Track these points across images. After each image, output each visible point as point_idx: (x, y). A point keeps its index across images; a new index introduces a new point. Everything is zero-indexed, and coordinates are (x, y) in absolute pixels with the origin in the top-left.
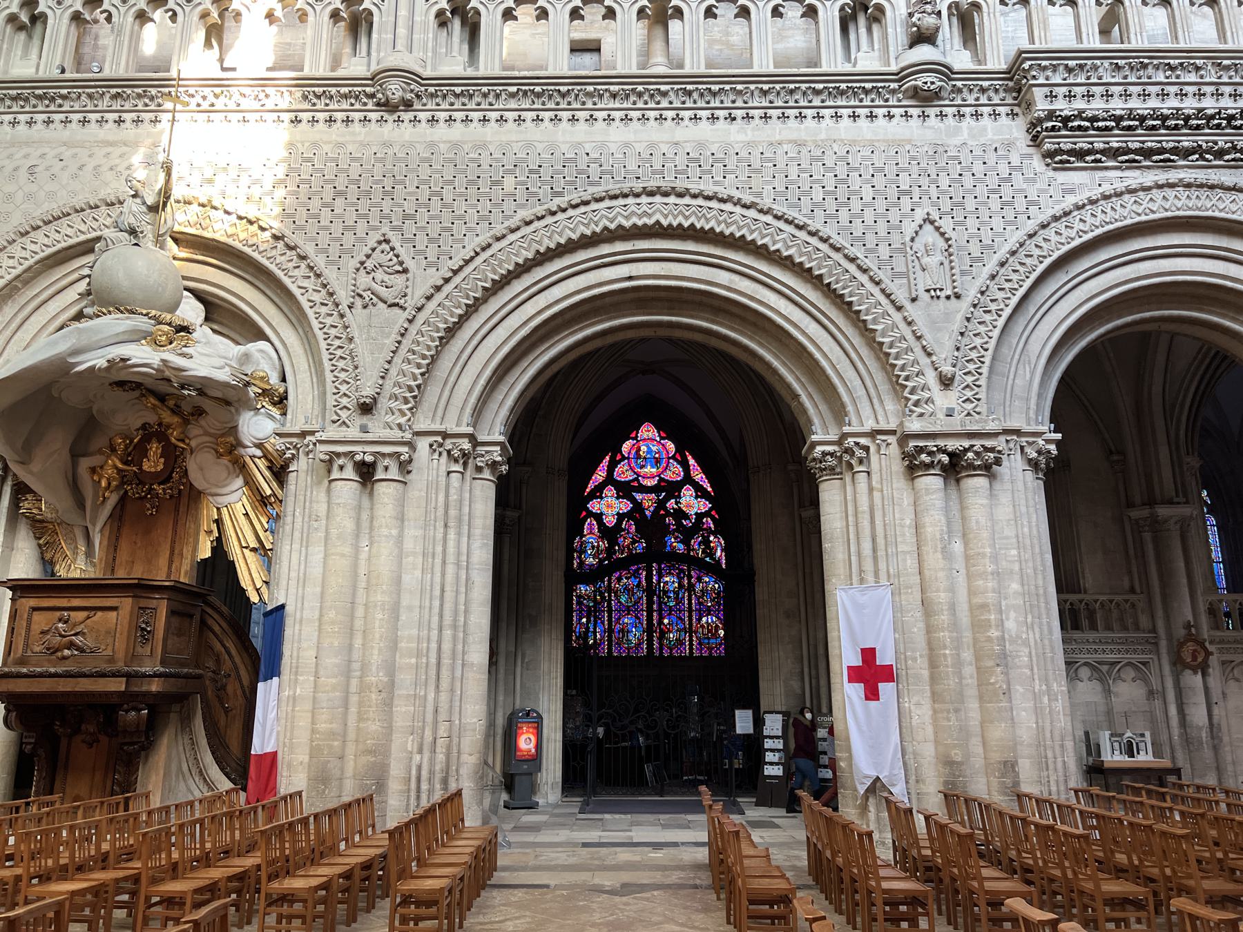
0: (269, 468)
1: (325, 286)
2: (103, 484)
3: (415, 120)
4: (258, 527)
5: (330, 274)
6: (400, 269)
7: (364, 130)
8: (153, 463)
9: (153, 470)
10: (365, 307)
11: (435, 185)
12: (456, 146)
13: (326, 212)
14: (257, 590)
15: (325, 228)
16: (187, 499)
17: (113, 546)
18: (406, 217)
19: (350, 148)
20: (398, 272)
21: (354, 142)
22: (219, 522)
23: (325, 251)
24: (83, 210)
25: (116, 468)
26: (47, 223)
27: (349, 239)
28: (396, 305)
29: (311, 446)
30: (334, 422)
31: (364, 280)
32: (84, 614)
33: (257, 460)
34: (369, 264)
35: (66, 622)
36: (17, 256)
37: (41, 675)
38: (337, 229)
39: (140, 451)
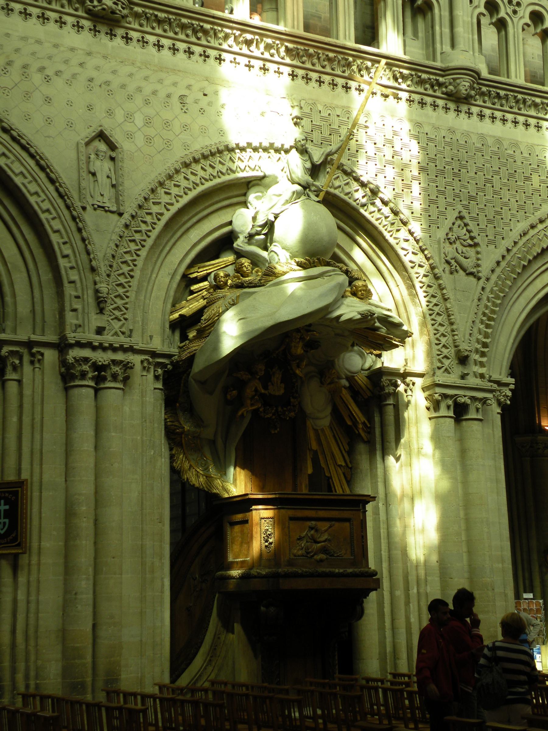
3: (470, 114)
6: (472, 243)
7: (434, 114)
9: (277, 394)
12: (499, 141)
18: (471, 198)
20: (470, 246)
21: (429, 124)
26: (205, 157)
28: (471, 274)
30: (439, 368)
31: (450, 249)
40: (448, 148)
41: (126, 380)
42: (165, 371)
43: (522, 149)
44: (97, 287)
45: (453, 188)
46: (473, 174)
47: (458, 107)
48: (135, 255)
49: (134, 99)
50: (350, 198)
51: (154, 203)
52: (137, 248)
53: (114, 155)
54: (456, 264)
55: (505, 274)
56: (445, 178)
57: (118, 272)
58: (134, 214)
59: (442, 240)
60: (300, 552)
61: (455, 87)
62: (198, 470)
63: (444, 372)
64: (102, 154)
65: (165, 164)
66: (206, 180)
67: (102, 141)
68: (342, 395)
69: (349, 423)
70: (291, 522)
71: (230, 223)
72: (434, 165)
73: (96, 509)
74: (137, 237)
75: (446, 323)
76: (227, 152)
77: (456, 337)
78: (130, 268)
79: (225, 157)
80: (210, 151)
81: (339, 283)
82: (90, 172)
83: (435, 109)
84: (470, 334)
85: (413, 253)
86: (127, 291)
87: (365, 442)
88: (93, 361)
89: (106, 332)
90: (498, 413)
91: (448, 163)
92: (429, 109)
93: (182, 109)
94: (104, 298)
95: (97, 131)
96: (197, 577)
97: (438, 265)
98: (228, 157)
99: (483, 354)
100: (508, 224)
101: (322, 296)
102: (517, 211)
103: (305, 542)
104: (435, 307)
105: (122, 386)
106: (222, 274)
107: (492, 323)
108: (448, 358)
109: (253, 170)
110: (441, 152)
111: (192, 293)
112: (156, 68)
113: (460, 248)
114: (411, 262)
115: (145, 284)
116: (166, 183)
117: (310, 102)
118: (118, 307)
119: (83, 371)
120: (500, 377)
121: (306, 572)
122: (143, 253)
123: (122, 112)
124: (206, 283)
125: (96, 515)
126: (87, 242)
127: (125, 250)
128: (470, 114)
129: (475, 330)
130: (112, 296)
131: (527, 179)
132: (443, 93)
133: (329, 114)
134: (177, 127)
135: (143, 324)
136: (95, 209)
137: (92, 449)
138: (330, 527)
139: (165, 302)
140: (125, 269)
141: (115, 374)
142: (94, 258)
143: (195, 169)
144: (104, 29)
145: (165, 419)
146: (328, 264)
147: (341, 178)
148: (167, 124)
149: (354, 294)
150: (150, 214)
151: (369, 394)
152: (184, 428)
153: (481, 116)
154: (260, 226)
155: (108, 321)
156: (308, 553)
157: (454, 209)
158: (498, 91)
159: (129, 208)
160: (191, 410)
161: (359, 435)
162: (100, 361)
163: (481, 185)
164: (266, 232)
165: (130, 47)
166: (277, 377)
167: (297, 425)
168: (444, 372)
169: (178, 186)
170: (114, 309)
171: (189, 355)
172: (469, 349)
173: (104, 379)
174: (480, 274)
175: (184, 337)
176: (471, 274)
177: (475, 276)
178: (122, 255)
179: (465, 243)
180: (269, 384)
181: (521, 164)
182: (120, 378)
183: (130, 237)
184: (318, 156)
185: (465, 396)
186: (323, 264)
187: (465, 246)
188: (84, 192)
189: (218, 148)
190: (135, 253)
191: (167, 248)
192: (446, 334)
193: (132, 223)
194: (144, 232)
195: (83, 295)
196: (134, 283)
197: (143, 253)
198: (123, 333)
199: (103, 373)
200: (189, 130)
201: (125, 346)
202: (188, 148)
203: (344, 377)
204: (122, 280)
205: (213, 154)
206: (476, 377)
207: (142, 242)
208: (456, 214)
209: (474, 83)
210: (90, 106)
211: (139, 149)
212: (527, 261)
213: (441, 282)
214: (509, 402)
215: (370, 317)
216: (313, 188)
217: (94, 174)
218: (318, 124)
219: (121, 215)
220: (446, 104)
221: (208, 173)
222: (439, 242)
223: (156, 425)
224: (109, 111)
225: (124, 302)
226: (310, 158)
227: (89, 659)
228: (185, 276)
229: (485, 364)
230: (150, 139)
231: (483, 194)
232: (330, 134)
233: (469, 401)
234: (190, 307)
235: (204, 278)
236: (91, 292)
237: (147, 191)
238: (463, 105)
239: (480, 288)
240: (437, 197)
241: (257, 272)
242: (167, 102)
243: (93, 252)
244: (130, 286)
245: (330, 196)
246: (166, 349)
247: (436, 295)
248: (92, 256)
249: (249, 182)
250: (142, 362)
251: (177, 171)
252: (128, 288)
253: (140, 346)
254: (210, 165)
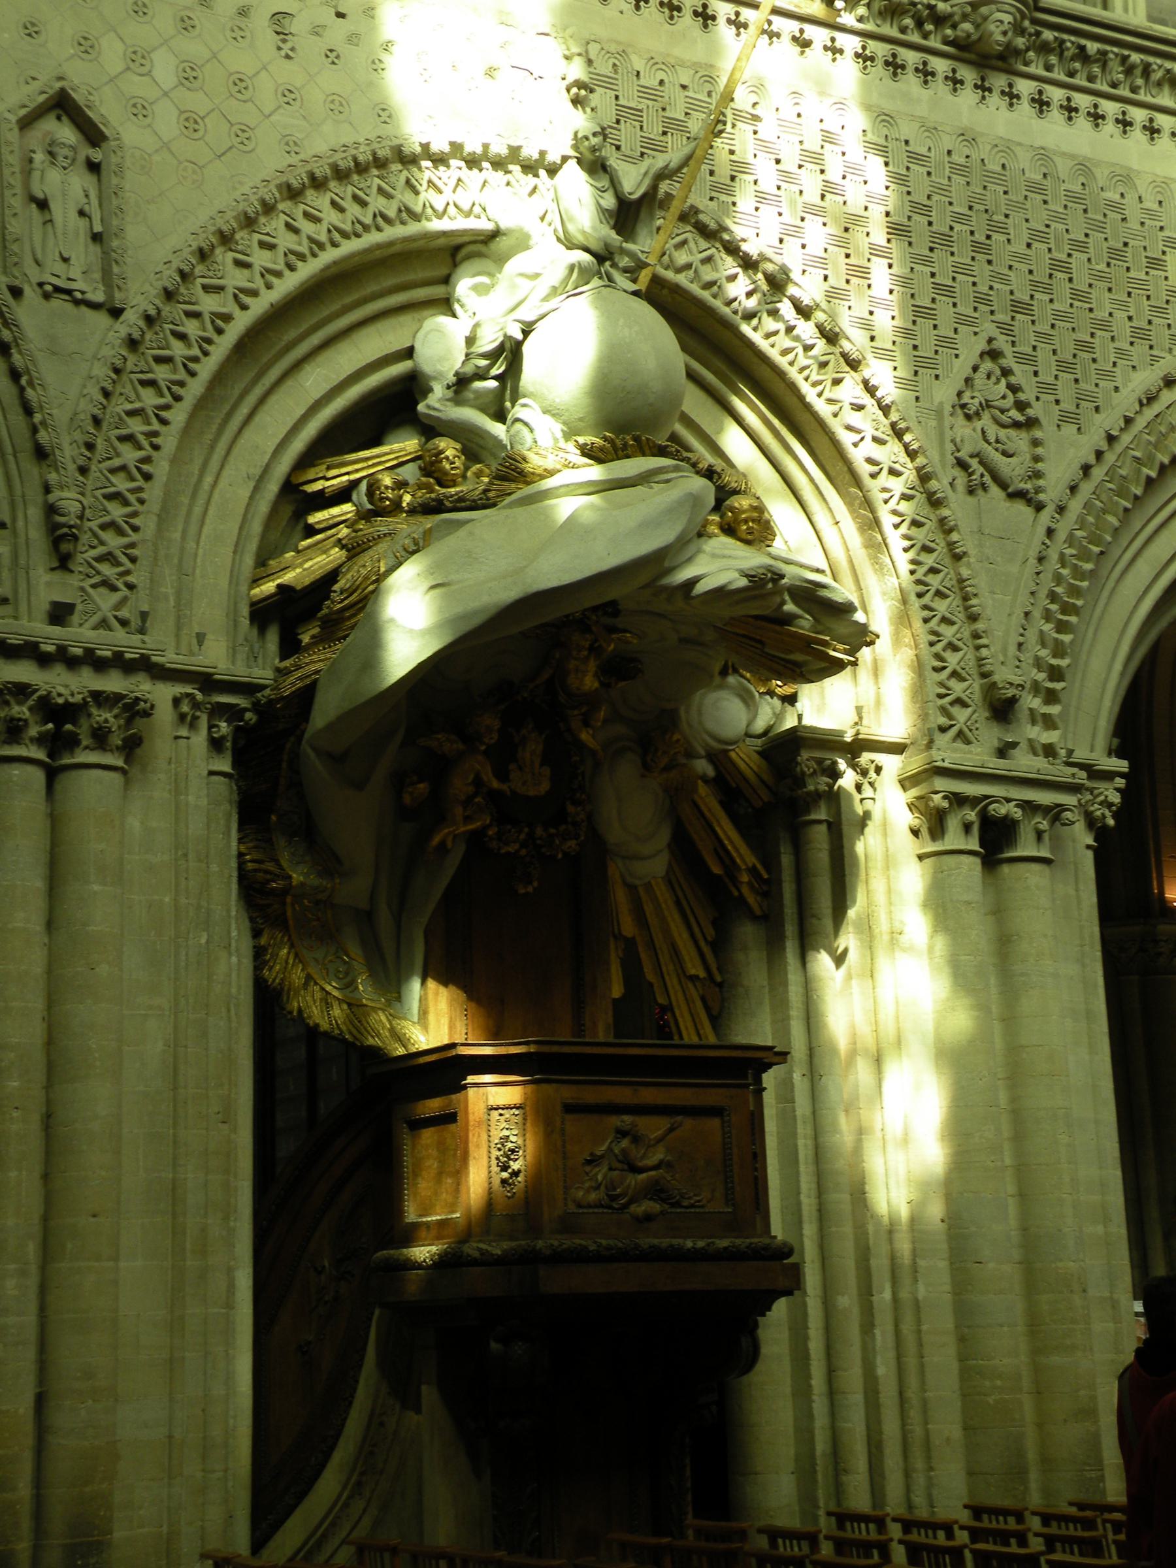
6: (1019, 417)
7: (925, 94)
9: (532, 793)
11: (1059, 250)
12: (1084, 167)
18: (1018, 307)
26: (341, 175)
28: (1019, 495)
30: (943, 730)
40: (958, 180)
41: (132, 746)
42: (238, 729)
43: (1142, 190)
44: (51, 498)
45: (972, 279)
46: (1022, 248)
47: (983, 79)
48: (154, 420)
49: (150, 13)
51: (206, 288)
52: (161, 401)
53: (97, 155)
54: (981, 469)
55: (1104, 497)
56: (952, 254)
57: (108, 463)
58: (152, 312)
59: (948, 409)
60: (593, 1197)
61: (977, 26)
62: (328, 988)
63: (954, 740)
64: (66, 151)
65: (234, 189)
66: (345, 235)
67: (64, 118)
68: (696, 798)
69: (717, 870)
70: (568, 1117)
71: (409, 353)
72: (925, 220)
73: (49, 1086)
74: (162, 373)
75: (959, 617)
76: (400, 167)
77: (984, 652)
78: (142, 454)
79: (392, 179)
80: (355, 159)
81: (691, 494)
82: (33, 199)
83: (926, 82)
84: (1020, 645)
85: (875, 439)
86: (135, 514)
87: (755, 918)
88: (42, 693)
89: (75, 618)
90: (1088, 847)
91: (959, 218)
92: (911, 81)
93: (279, 49)
94: (71, 527)
95: (51, 92)
96: (326, 1264)
97: (939, 469)
98: (402, 179)
99: (1051, 697)
100: (1107, 375)
101: (647, 525)
102: (1132, 343)
103: (605, 1169)
104: (931, 576)
105: (120, 762)
106: (387, 481)
107: (1073, 619)
108: (964, 705)
109: (468, 214)
110: (944, 190)
111: (311, 531)
113: (993, 431)
114: (870, 461)
115: (185, 500)
116: (238, 236)
117: (613, 48)
118: (110, 553)
119: (12, 719)
120: (1094, 756)
121: (609, 1248)
122: (178, 415)
123: (119, 47)
124: (347, 507)
125: (49, 1102)
126: (23, 381)
127: (129, 407)
128: (1012, 97)
129: (1032, 636)
130: (94, 525)
131: (1155, 263)
132: (946, 42)
133: (661, 82)
134: (265, 92)
135: (178, 605)
136: (47, 296)
137: (36, 925)
138: (671, 1130)
139: (237, 549)
140: (129, 455)
141: (100, 728)
142: (43, 423)
143: (314, 204)
145: (240, 855)
146: (662, 452)
147: (692, 244)
148: (239, 84)
149: (729, 530)
150: (196, 315)
151: (765, 796)
152: (290, 877)
153: (1041, 104)
154: (484, 356)
155: (82, 589)
156: (613, 1198)
157: (976, 334)
158: (1083, 42)
159: (140, 296)
160: (308, 834)
161: (742, 900)
162: (60, 695)
163: (1041, 276)
164: (500, 371)
166: (532, 748)
167: (583, 872)
168: (954, 740)
169: (271, 247)
170: (99, 559)
171: (300, 685)
172: (1018, 680)
173: (72, 742)
174: (1042, 497)
175: (290, 647)
176: (1019, 495)
177: (1029, 502)
178: (121, 419)
179: (1004, 418)
180: (512, 766)
181: (1139, 227)
182: (116, 740)
183: (142, 372)
184: (633, 181)
185: (1008, 800)
186: (648, 452)
187: (1004, 426)
188: (15, 247)
189: (374, 154)
190: (157, 416)
191: (244, 410)
192: (960, 644)
193: (148, 336)
194: (178, 360)
195: (14, 519)
196: (154, 492)
197: (178, 415)
198: (124, 623)
199: (69, 727)
200: (298, 103)
201: (128, 656)
202: (296, 149)
203: (703, 752)
204: (121, 484)
205: (361, 169)
206: (1035, 754)
207: (175, 388)
208: (981, 345)
209: (1023, 16)
210: (33, 25)
211: (166, 146)
212: (1157, 466)
213: (945, 512)
214: (1111, 822)
215: (770, 585)
216: (625, 262)
217: (43, 205)
218: (632, 105)
219: (116, 313)
220: (954, 71)
221: (349, 216)
222: (939, 413)
223: (214, 868)
224: (82, 41)
225: (125, 540)
226: (615, 184)
227: (24, 1490)
228: (290, 488)
229: (1057, 720)
230: (196, 122)
231: (1047, 298)
232: (665, 133)
233: (1018, 814)
234: (306, 566)
235: (343, 495)
236: (35, 513)
237: (186, 254)
238: (996, 74)
239: (1041, 531)
240: (933, 300)
241: (478, 475)
242: (240, 29)
243: (41, 407)
244: (142, 502)
245: (665, 292)
246: (241, 671)
247: (932, 545)
248: (37, 418)
249: (457, 248)
250: (176, 701)
251: (268, 208)
252: (138, 507)
253: (170, 658)
254: (356, 198)
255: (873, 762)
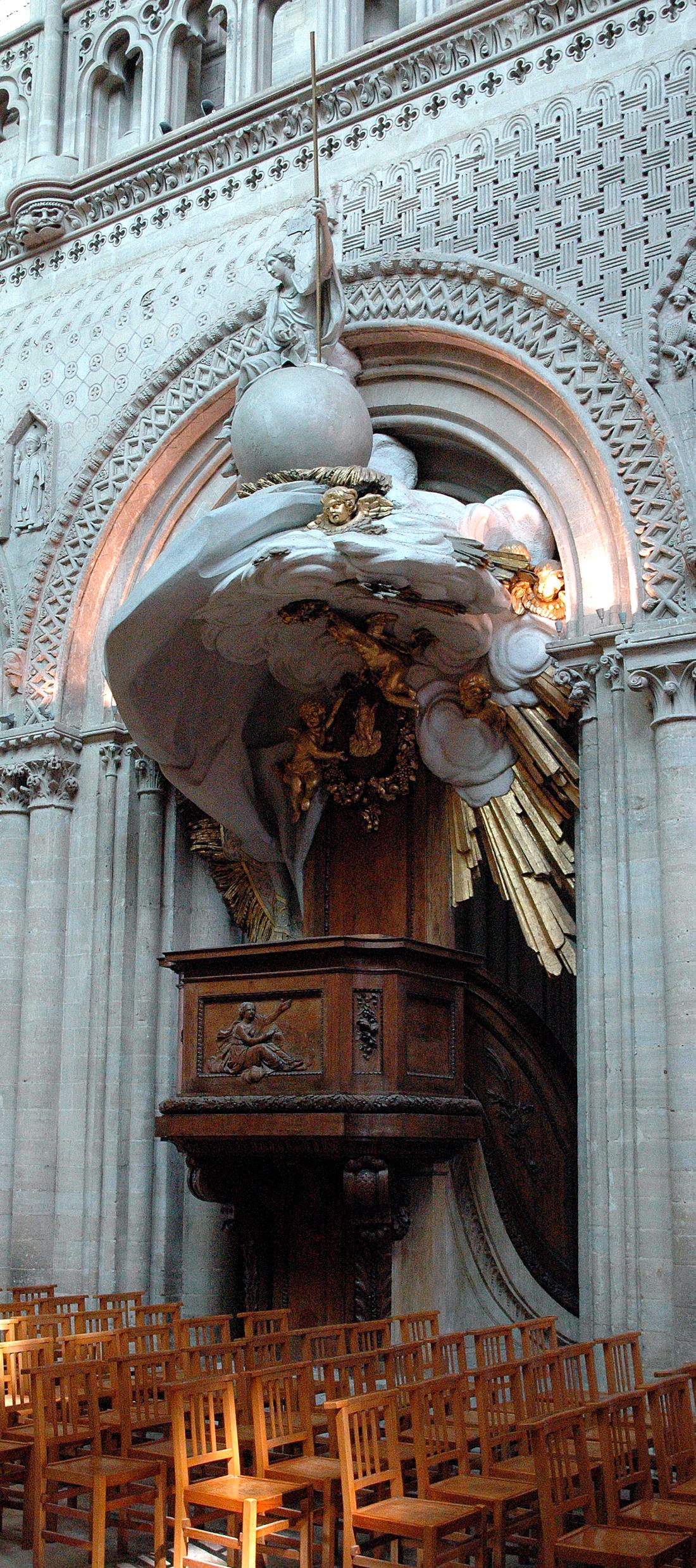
0: (552, 723)
1: (601, 357)
2: (298, 784)
4: (546, 835)
5: (611, 331)
8: (367, 742)
9: (366, 754)
10: (680, 375)
13: (591, 221)
14: (557, 951)
15: (593, 248)
16: (426, 803)
17: (321, 891)
19: (620, 84)
22: (480, 832)
23: (596, 290)
24: (218, 339)
25: (312, 758)
26: (174, 375)
27: (637, 254)
29: (614, 667)
32: (275, 1005)
33: (530, 712)
34: (680, 291)
35: (250, 1020)
36: (140, 439)
37: (223, 1110)
38: (612, 245)
39: (345, 727)
50: (442, 319)
72: (638, 152)
85: (585, 369)
98: (216, 355)
105: (63, 803)
112: (112, 273)
136: (19, 535)
140: (53, 611)
144: (46, 258)
165: (81, 262)
203: (517, 686)
204: (47, 632)
205: (189, 362)
255: (612, 656)
